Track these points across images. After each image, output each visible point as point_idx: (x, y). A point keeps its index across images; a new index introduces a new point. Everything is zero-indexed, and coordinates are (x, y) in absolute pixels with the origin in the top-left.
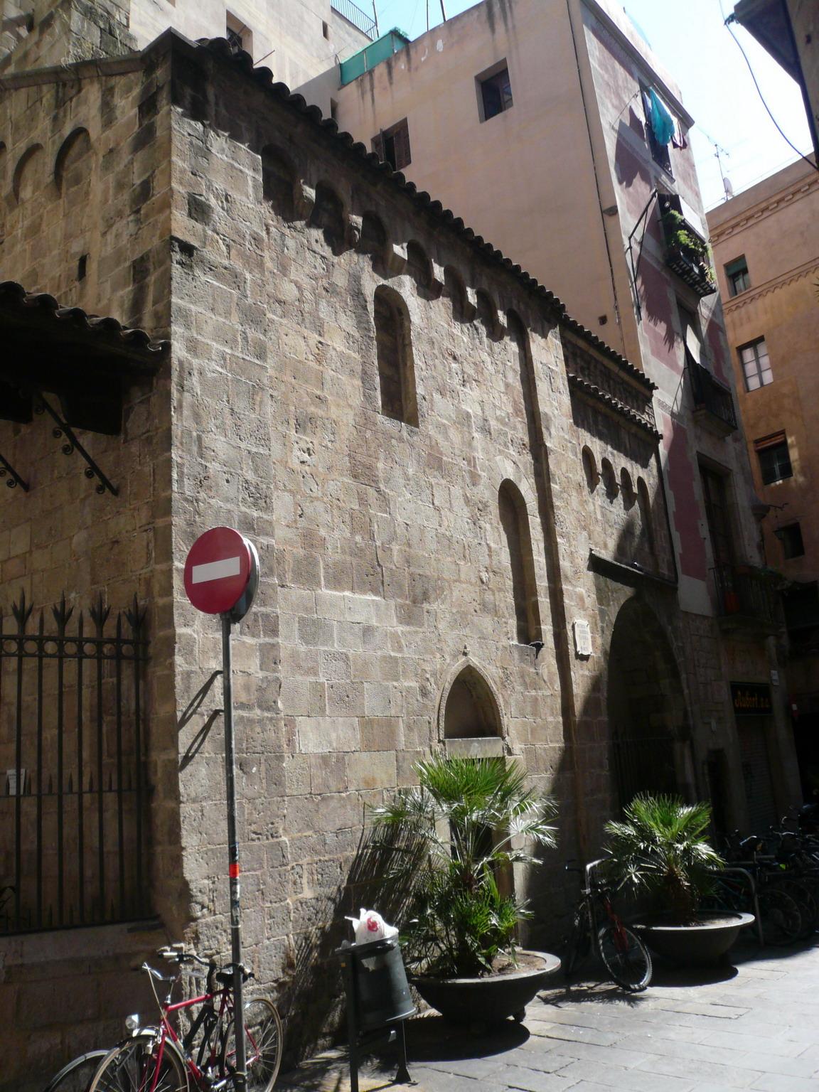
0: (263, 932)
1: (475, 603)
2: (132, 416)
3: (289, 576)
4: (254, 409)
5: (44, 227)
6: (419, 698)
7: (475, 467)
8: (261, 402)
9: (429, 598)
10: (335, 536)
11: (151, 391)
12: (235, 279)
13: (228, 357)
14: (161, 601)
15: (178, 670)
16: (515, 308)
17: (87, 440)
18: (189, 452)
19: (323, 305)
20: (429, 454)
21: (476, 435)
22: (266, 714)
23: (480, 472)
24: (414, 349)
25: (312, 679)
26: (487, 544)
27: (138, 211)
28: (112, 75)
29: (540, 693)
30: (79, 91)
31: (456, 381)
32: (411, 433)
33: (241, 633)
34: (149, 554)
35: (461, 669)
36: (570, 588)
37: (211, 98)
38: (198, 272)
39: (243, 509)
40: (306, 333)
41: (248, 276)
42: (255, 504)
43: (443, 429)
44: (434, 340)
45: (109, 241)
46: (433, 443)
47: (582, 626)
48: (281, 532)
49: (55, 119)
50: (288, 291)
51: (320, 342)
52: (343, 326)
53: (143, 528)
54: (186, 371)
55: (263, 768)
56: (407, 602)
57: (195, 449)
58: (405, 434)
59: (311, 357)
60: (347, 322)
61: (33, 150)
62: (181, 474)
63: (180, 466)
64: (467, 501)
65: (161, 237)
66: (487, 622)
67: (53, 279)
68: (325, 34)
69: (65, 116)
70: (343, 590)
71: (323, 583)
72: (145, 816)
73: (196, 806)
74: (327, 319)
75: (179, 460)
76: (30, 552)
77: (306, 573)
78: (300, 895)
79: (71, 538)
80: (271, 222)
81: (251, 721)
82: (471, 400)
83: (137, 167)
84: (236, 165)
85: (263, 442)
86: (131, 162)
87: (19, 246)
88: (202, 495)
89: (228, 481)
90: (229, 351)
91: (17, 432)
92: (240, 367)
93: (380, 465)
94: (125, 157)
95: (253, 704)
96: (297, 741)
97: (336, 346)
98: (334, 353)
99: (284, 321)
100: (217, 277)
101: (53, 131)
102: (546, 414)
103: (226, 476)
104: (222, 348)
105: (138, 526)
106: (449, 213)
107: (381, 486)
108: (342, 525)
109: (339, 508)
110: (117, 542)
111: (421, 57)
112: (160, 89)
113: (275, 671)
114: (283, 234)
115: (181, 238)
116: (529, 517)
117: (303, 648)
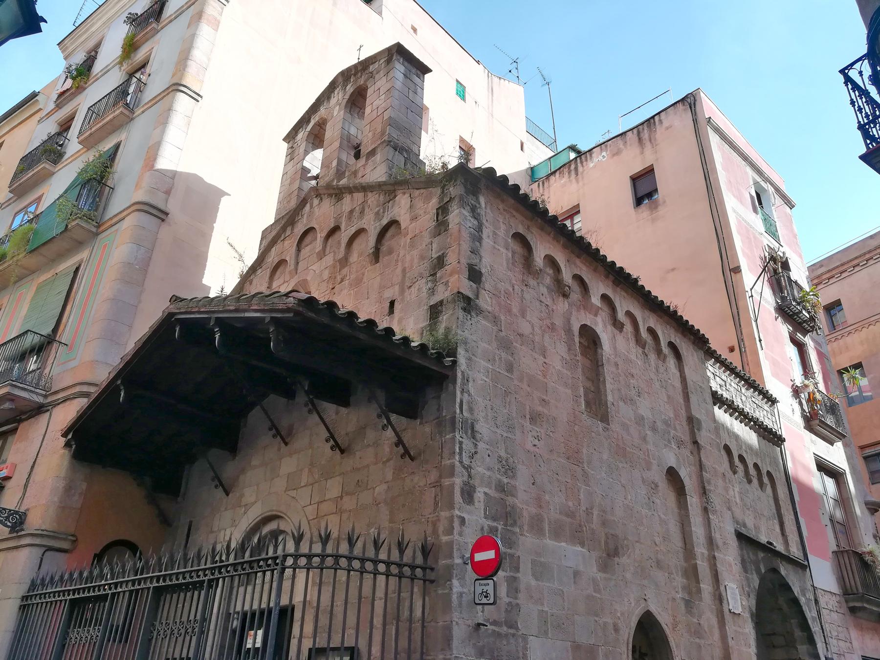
1: (651, 561)
3: (526, 528)
4: (505, 406)
5: (365, 280)
7: (648, 455)
10: (556, 500)
11: (442, 390)
12: (495, 320)
14: (444, 539)
15: (455, 590)
18: (466, 433)
19: (547, 336)
20: (617, 444)
21: (648, 432)
22: (512, 631)
23: (652, 461)
27: (434, 275)
30: (395, 196)
31: (633, 392)
36: (722, 556)
40: (536, 356)
41: (503, 318)
42: (506, 473)
43: (625, 427)
44: (619, 363)
45: (413, 291)
46: (620, 437)
47: (733, 589)
48: (521, 495)
50: (526, 329)
51: (545, 363)
53: (432, 486)
57: (470, 432)
59: (539, 373)
60: (562, 349)
61: (360, 232)
62: (461, 449)
63: (461, 443)
64: (644, 481)
65: (451, 291)
66: (660, 576)
69: (384, 212)
76: (341, 497)
77: (537, 525)
79: (374, 489)
81: (499, 635)
82: (644, 408)
85: (511, 429)
88: (473, 465)
89: (489, 456)
93: (584, 451)
94: (427, 240)
98: (553, 370)
99: (523, 348)
101: (374, 221)
105: (429, 483)
107: (586, 468)
112: (451, 199)
113: (516, 598)
114: (522, 290)
116: (688, 497)
117: (533, 582)
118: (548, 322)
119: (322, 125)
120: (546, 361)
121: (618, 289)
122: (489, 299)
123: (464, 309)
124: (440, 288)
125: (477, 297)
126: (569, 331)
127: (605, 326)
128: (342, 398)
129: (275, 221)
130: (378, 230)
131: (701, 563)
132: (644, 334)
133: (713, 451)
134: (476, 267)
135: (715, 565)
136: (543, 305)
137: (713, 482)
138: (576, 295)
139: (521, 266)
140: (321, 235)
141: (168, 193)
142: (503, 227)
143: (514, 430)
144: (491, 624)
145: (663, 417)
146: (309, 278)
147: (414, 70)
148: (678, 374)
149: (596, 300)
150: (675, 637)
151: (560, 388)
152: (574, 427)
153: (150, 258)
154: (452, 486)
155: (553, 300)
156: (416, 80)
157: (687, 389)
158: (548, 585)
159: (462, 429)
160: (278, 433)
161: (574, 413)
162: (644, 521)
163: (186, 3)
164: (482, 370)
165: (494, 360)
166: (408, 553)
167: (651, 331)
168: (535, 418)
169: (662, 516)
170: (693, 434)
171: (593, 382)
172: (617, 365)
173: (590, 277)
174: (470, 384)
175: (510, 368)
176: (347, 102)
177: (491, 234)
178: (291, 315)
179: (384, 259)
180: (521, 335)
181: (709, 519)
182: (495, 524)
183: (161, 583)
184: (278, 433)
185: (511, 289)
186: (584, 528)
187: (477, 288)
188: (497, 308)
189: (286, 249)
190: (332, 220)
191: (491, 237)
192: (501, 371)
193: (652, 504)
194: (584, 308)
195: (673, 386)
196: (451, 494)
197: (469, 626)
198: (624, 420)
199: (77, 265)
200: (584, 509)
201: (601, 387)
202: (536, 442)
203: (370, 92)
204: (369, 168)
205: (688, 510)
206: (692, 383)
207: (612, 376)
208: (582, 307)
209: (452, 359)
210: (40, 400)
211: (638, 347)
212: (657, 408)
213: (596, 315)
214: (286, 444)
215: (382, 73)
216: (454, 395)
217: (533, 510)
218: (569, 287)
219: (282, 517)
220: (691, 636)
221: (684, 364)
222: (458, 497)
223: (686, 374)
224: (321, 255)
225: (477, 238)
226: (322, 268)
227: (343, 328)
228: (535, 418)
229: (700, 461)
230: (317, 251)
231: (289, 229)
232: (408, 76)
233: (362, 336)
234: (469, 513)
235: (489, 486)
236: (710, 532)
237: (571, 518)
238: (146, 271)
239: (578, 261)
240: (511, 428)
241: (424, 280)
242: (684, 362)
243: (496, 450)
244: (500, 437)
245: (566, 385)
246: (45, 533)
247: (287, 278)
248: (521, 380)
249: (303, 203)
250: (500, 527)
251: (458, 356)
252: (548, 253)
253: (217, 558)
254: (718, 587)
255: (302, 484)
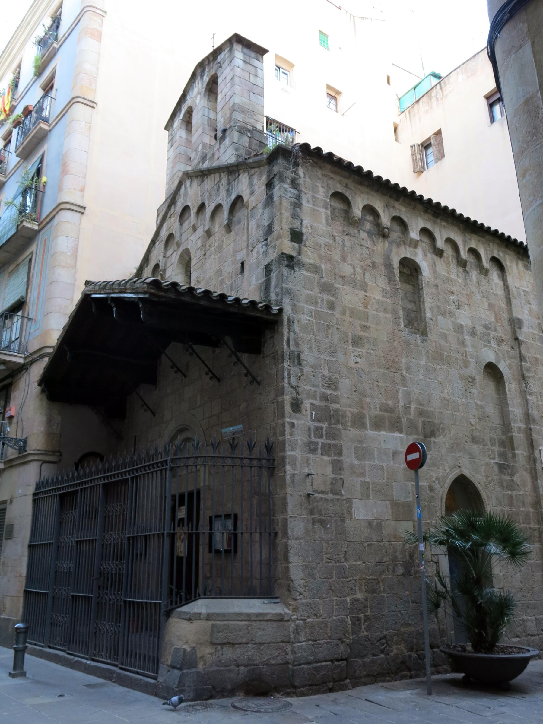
0: (333, 613)
1: (466, 438)
2: (266, 345)
5: (224, 246)
6: (428, 492)
7: (466, 356)
8: (332, 333)
9: (435, 434)
11: (274, 332)
12: (316, 269)
13: (313, 311)
14: (281, 438)
15: (288, 473)
16: (496, 255)
17: (245, 357)
18: (293, 362)
19: (367, 275)
21: (467, 337)
23: (470, 359)
24: (424, 291)
25: (363, 479)
26: (475, 402)
27: (266, 240)
28: (253, 168)
29: (514, 493)
30: (239, 175)
32: (423, 340)
33: (322, 454)
34: (274, 414)
35: (456, 476)
37: (302, 175)
38: (296, 269)
39: (323, 390)
40: (357, 292)
41: (323, 267)
42: (328, 387)
43: (444, 336)
46: (438, 345)
49: (228, 191)
50: (347, 270)
51: (366, 296)
52: (380, 284)
54: (290, 322)
55: (333, 525)
56: (420, 437)
57: (296, 361)
58: (419, 342)
59: (361, 305)
60: (382, 282)
61: (219, 207)
62: (289, 375)
63: (289, 370)
64: (461, 377)
65: (277, 253)
66: (475, 448)
67: (229, 273)
68: (389, 83)
69: (232, 189)
70: (381, 431)
71: (368, 427)
72: (273, 545)
73: (297, 542)
74: (370, 283)
75: (288, 367)
78: (354, 596)
79: (240, 406)
80: (336, 234)
81: (326, 500)
83: (266, 216)
84: (316, 208)
85: (333, 354)
86: (263, 214)
87: (213, 256)
88: (300, 384)
89: (314, 376)
90: (314, 308)
91: (214, 352)
92: (319, 315)
93: (403, 360)
94: (261, 211)
95: (328, 492)
96: (353, 512)
97: (374, 296)
98: (374, 301)
99: (345, 287)
100: (308, 270)
101: (227, 197)
102: (519, 319)
103: (313, 373)
104: (310, 307)
106: (446, 207)
107: (404, 372)
108: (380, 396)
109: (378, 386)
110: (260, 408)
111: (450, 86)
112: (275, 175)
114: (343, 240)
115: (287, 253)
116: (506, 384)
117: (356, 462)
118: (369, 262)
119: (190, 112)
120: (366, 294)
121: (438, 220)
122: (310, 254)
123: (288, 266)
124: (271, 251)
125: (299, 254)
126: (389, 266)
127: (425, 255)
128: (215, 343)
129: (166, 200)
130: (229, 204)
131: (517, 435)
132: (464, 254)
133: (535, 344)
134: (297, 230)
135: (531, 435)
136: (364, 248)
137: (533, 369)
138: (395, 235)
139: (341, 219)
140: (193, 211)
141: (82, 190)
142: (321, 190)
143: (335, 354)
144: (319, 493)
145: (483, 322)
146: (189, 247)
147: (253, 54)
148: (501, 283)
149: (414, 235)
150: (487, 491)
151: (380, 314)
152: (393, 343)
153: (78, 245)
154: (283, 402)
155: (374, 242)
156: (256, 63)
157: (509, 295)
158: (370, 463)
159: (289, 359)
160: (179, 370)
161: (393, 333)
162: (461, 408)
163: (74, 21)
164: (305, 312)
165: (317, 302)
166: (256, 451)
167: (473, 252)
168: (357, 341)
169: (479, 402)
170: (514, 332)
171: (415, 303)
172: (436, 286)
173: (409, 215)
174: (295, 325)
175: (331, 306)
176: (206, 91)
177: (310, 199)
178: (147, 296)
179: (236, 228)
180: (343, 277)
181: (527, 400)
182: (320, 425)
183: (106, 481)
184: (179, 370)
185: (331, 242)
186: (403, 419)
187: (300, 247)
188: (318, 260)
189: (173, 224)
190: (200, 198)
191: (311, 201)
192: (324, 310)
193: (469, 394)
194: (404, 244)
195: (495, 295)
196: (283, 407)
197: (301, 496)
198: (442, 331)
199: (30, 257)
200: (402, 404)
201: (422, 306)
202: (358, 360)
203: (220, 81)
204: (222, 150)
205: (506, 395)
206: (514, 289)
207: (431, 297)
208: (402, 243)
209: (278, 308)
210: (21, 361)
211: (459, 267)
212: (477, 316)
213: (416, 247)
214: (185, 376)
215: (227, 63)
216: (282, 334)
217: (356, 411)
218: (388, 229)
219: (187, 429)
220: (503, 489)
221: (507, 274)
222: (288, 408)
223: (509, 282)
224: (194, 229)
225: (297, 204)
226: (197, 238)
227: (187, 299)
228: (357, 341)
229: (520, 353)
230: (192, 224)
231: (173, 207)
232: (248, 61)
233: (203, 302)
234: (297, 419)
235: (315, 398)
236: (528, 410)
237: (391, 413)
238: (76, 256)
239: (397, 204)
240: (333, 353)
241: (260, 245)
242: (506, 271)
243: (320, 371)
244: (323, 361)
245: (386, 311)
246: (39, 452)
247: (176, 248)
248: (343, 313)
249: (180, 184)
250: (324, 426)
251: (284, 305)
252: (366, 203)
253: (135, 463)
254: (533, 452)
255: (198, 405)
